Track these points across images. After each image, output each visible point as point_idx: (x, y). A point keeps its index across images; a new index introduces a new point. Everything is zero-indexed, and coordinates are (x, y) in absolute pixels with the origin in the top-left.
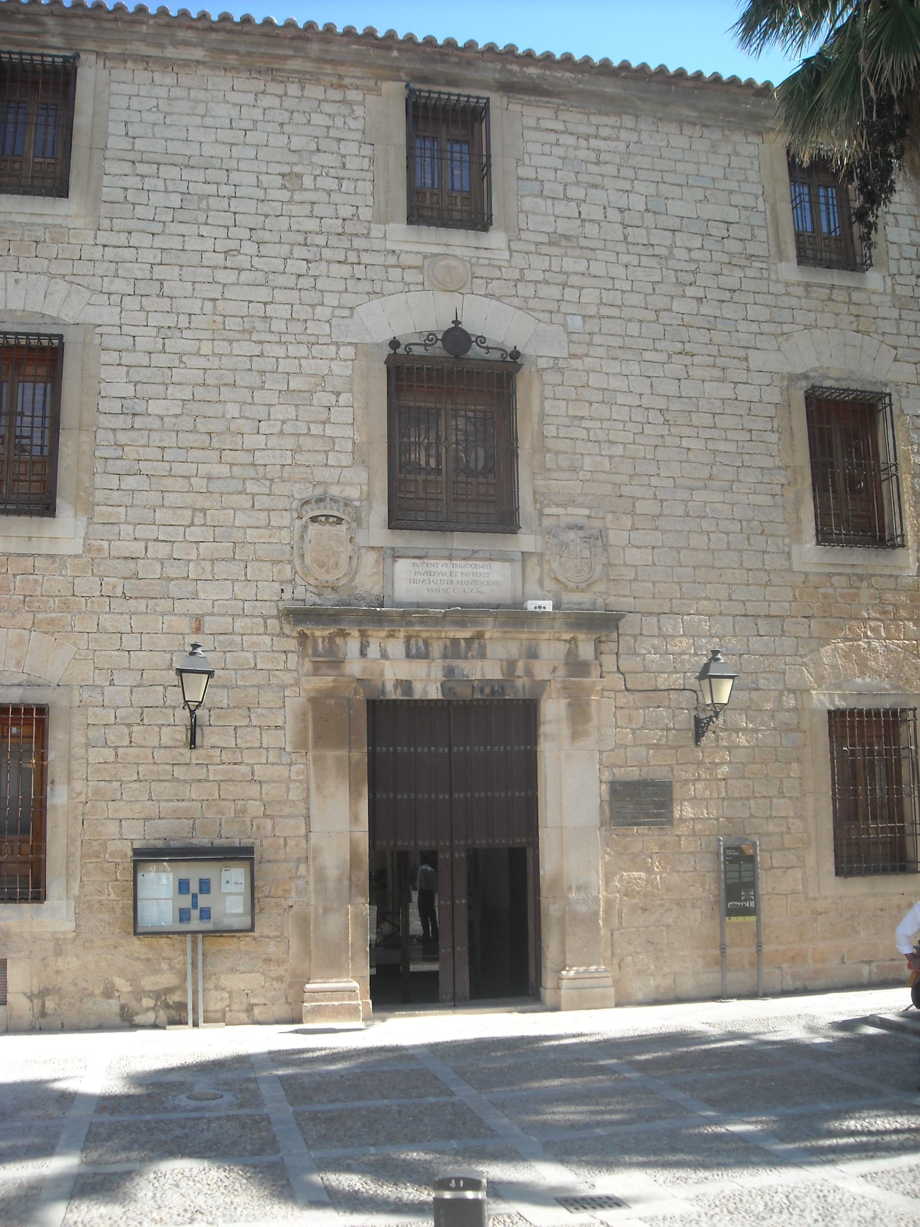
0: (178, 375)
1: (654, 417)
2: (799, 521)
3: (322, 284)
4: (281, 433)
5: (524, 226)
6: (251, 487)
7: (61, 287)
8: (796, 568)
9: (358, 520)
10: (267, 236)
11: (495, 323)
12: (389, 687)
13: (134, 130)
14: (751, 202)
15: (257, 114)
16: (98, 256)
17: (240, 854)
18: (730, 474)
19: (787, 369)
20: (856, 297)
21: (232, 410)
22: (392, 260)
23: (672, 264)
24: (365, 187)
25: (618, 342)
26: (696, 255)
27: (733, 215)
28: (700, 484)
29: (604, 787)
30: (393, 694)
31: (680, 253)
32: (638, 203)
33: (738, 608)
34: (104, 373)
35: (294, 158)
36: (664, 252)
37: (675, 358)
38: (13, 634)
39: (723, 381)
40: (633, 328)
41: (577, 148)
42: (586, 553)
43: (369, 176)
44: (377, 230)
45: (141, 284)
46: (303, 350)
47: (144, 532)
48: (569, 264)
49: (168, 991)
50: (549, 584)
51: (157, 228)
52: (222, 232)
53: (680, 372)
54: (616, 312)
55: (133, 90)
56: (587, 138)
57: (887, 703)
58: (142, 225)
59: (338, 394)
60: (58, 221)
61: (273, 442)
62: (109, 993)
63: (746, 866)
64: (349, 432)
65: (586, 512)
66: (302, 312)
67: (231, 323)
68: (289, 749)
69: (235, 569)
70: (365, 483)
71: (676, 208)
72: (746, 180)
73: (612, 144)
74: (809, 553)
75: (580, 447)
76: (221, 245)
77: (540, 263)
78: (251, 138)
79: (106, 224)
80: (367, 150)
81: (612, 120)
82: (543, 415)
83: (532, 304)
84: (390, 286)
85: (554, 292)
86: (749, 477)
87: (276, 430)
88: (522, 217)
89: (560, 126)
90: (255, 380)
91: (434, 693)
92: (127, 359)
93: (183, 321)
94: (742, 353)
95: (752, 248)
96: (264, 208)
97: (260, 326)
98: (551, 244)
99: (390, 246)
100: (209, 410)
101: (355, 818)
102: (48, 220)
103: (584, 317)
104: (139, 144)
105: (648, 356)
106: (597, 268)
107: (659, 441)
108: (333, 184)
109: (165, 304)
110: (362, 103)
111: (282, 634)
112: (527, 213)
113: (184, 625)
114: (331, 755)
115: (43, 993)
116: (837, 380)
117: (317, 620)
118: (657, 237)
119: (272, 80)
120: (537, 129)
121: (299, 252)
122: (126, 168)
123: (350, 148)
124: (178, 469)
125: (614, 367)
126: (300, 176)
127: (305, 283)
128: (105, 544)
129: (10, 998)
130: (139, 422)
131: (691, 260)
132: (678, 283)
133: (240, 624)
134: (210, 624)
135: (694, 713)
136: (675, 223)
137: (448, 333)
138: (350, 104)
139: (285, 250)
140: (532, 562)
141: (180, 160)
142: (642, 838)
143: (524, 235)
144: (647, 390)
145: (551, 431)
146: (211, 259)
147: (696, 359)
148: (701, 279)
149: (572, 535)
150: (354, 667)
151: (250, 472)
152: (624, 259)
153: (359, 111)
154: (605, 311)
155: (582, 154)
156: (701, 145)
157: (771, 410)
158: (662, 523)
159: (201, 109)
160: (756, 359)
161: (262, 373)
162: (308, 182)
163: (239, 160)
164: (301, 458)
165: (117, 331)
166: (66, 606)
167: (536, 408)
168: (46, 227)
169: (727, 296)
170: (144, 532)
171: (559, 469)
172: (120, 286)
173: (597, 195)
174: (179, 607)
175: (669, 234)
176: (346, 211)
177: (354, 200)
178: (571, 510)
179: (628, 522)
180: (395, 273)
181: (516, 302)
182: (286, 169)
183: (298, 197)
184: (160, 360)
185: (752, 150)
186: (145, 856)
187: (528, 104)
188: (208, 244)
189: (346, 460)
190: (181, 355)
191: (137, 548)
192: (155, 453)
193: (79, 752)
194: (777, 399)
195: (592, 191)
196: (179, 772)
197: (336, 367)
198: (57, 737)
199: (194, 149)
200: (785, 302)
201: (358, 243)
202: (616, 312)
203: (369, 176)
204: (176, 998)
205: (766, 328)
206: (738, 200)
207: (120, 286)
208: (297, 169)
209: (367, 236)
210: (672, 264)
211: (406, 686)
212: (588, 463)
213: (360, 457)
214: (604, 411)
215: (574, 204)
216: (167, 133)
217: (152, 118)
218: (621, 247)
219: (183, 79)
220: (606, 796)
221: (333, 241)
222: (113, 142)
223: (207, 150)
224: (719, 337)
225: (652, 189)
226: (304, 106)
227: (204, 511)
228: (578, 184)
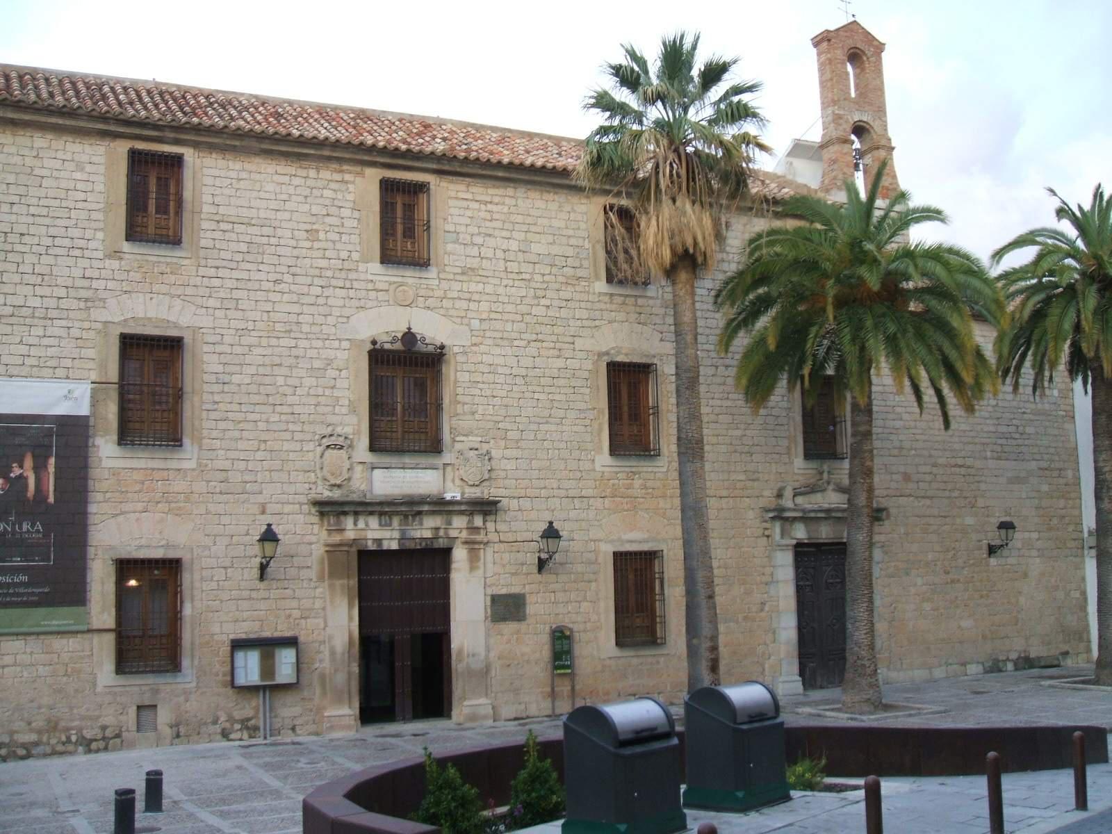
0: (248, 359)
1: (519, 381)
2: (600, 440)
3: (330, 301)
4: (309, 394)
5: (446, 262)
6: (291, 427)
7: (178, 302)
8: (597, 469)
9: (351, 446)
10: (298, 271)
11: (432, 328)
12: (370, 543)
13: (217, 200)
14: (580, 242)
15: (291, 190)
16: (199, 284)
17: (292, 642)
18: (561, 413)
19: (597, 348)
20: (640, 301)
21: (280, 381)
22: (370, 286)
23: (533, 285)
24: (355, 239)
25: (499, 335)
26: (547, 278)
27: (570, 252)
28: (544, 420)
29: (489, 599)
30: (371, 546)
31: (538, 278)
32: (514, 246)
33: (563, 493)
34: (206, 358)
35: (314, 219)
36: (527, 276)
37: (533, 344)
38: (158, 516)
39: (558, 357)
40: (509, 327)
41: (479, 210)
42: (479, 465)
43: (357, 231)
44: (362, 267)
45: (225, 301)
46: (319, 344)
47: (232, 455)
48: (473, 287)
49: (249, 719)
50: (458, 482)
51: (234, 265)
52: (272, 268)
53: (534, 352)
54: (498, 316)
55: (217, 173)
56: (486, 203)
57: (645, 547)
58: (224, 264)
59: (341, 370)
60: (175, 260)
61: (304, 400)
62: (215, 722)
63: (565, 642)
64: (347, 393)
65: (480, 439)
66: (320, 320)
67: (278, 327)
68: (314, 580)
69: (284, 477)
70: (356, 425)
71: (535, 248)
72: (579, 229)
73: (499, 208)
74: (604, 459)
75: (477, 400)
76: (272, 277)
77: (456, 286)
78: (289, 206)
79: (203, 262)
80: (356, 214)
81: (500, 191)
82: (456, 381)
83: (452, 312)
84: (370, 304)
85: (464, 304)
86: (572, 415)
87: (305, 393)
88: (446, 256)
89: (469, 196)
90: (292, 361)
91: (394, 546)
92: (219, 348)
93: (250, 325)
94: (570, 340)
95: (580, 273)
96: (296, 252)
97: (294, 328)
98: (463, 273)
99: (370, 277)
100: (267, 380)
101: (351, 618)
102: (169, 260)
103: (481, 320)
104: (222, 210)
105: (516, 343)
106: (489, 289)
107: (521, 395)
108: (336, 237)
109: (239, 314)
110: (353, 182)
111: (310, 514)
112: (449, 254)
113: (256, 509)
114: (338, 583)
115: (177, 725)
116: (626, 355)
117: (331, 509)
118: (527, 268)
119: (300, 167)
120: (456, 198)
121: (317, 281)
122: (213, 225)
123: (346, 212)
124: (251, 417)
125: (497, 351)
126: (317, 231)
127: (321, 301)
128: (209, 462)
129: (159, 727)
130: (226, 388)
131: (544, 282)
132: (536, 297)
133: (287, 509)
134: (270, 508)
135: (537, 555)
136: (533, 258)
137: (405, 335)
138: (347, 182)
139: (309, 280)
140: (449, 469)
141: (246, 220)
142: (509, 627)
143: (447, 269)
144: (515, 365)
145: (460, 391)
146: (266, 286)
147: (544, 344)
148: (549, 294)
149: (472, 453)
150: (350, 535)
151: (291, 418)
152: (505, 282)
153: (351, 187)
154: (493, 316)
155: (482, 214)
156: (553, 206)
157: (586, 375)
158: (522, 444)
159: (257, 187)
160: (579, 343)
161: (297, 357)
162: (322, 235)
163: (281, 221)
164: (321, 409)
165: (212, 331)
166: (187, 500)
167: (452, 378)
168: (168, 264)
169: (564, 304)
170: (232, 455)
171: (464, 414)
172: (211, 303)
173: (491, 242)
174: (252, 498)
175: (531, 265)
176: (344, 255)
177: (350, 247)
178: (470, 438)
179: (502, 443)
180: (372, 294)
181: (442, 311)
182: (308, 227)
183: (316, 245)
184: (238, 350)
185: (583, 208)
186: (238, 645)
187: (452, 182)
188: (262, 276)
189: (344, 410)
190: (250, 346)
191: (227, 465)
192: (235, 407)
193: (197, 584)
194: (590, 367)
195: (487, 238)
196: (254, 594)
197: (339, 354)
198: (186, 577)
199: (253, 213)
200: (598, 306)
201: (353, 275)
202: (498, 316)
203: (357, 231)
204: (253, 722)
205: (586, 323)
206: (573, 241)
207: (211, 303)
208: (315, 227)
209: (357, 271)
210: (533, 285)
211: (378, 541)
212: (480, 410)
213: (353, 410)
214: (491, 377)
215: (476, 248)
216: (239, 202)
217: (227, 191)
218: (503, 275)
219: (247, 166)
220: (489, 603)
221: (337, 274)
222: (206, 208)
223: (262, 214)
224: (557, 330)
225: (522, 236)
226: (320, 184)
227: (265, 441)
228: (479, 234)
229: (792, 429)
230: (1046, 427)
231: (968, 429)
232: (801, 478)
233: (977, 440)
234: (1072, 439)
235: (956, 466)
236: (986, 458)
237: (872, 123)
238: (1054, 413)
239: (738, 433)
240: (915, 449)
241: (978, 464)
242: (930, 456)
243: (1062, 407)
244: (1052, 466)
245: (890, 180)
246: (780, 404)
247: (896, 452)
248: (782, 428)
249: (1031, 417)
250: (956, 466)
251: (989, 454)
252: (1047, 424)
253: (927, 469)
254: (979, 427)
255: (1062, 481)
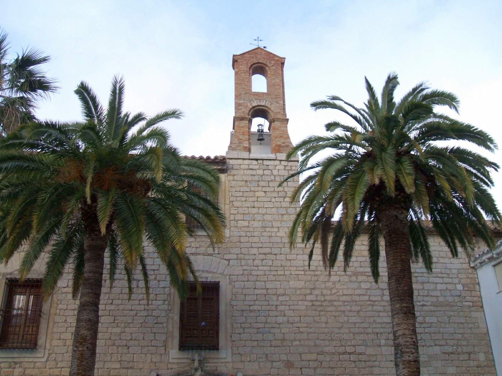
229: (170, 326)
230: (450, 317)
231: (359, 320)
232: (175, 366)
233: (370, 330)
234: (482, 325)
235: (345, 353)
236: (379, 346)
237: (269, 106)
238: (459, 304)
239: (118, 330)
240: (299, 340)
241: (370, 351)
242: (316, 346)
243: (468, 298)
244: (460, 350)
245: (283, 140)
246: (161, 307)
247: (279, 343)
248: (161, 325)
249: (433, 308)
250: (345, 353)
251: (383, 342)
252: (452, 313)
253: (314, 356)
254: (372, 320)
255: (471, 363)
